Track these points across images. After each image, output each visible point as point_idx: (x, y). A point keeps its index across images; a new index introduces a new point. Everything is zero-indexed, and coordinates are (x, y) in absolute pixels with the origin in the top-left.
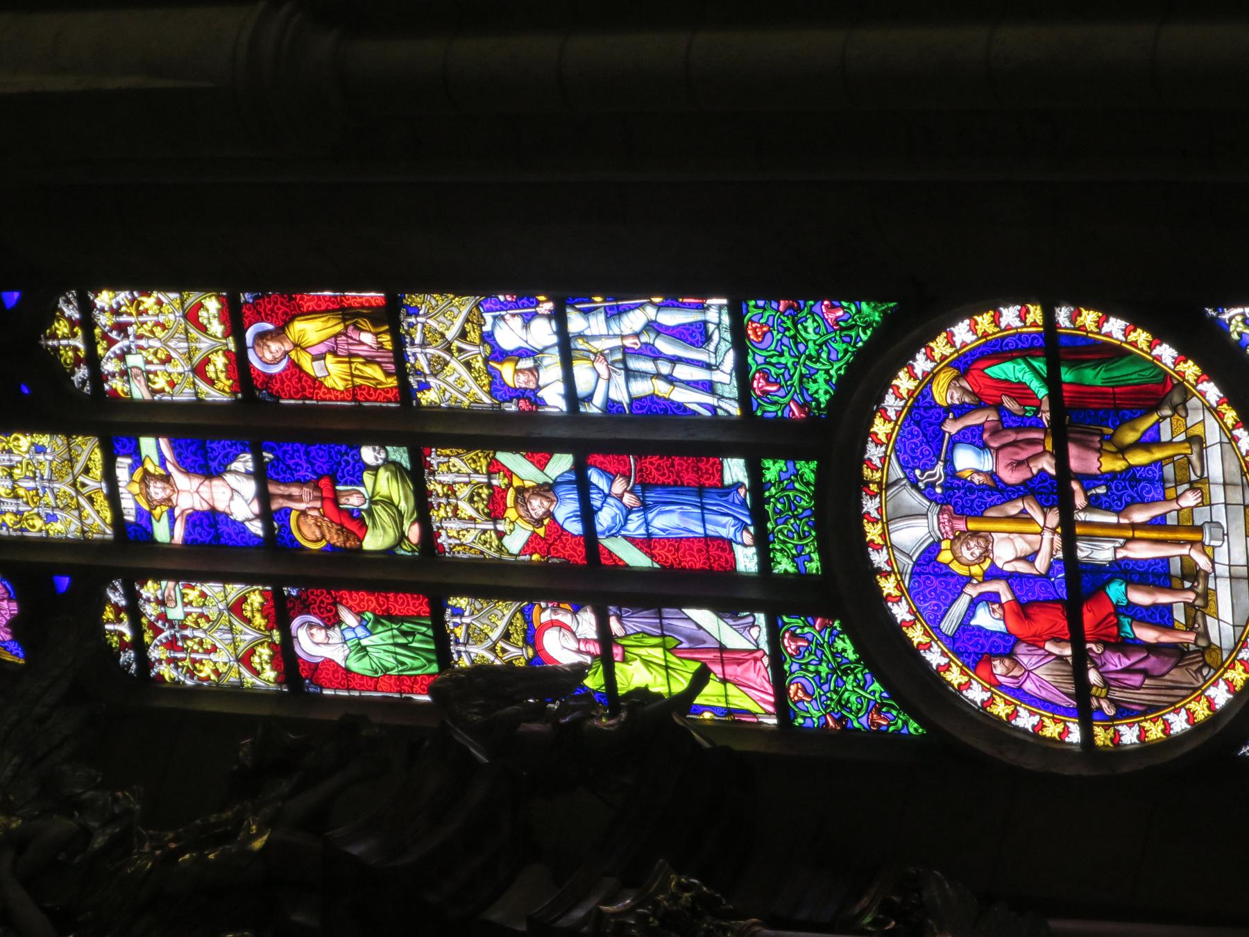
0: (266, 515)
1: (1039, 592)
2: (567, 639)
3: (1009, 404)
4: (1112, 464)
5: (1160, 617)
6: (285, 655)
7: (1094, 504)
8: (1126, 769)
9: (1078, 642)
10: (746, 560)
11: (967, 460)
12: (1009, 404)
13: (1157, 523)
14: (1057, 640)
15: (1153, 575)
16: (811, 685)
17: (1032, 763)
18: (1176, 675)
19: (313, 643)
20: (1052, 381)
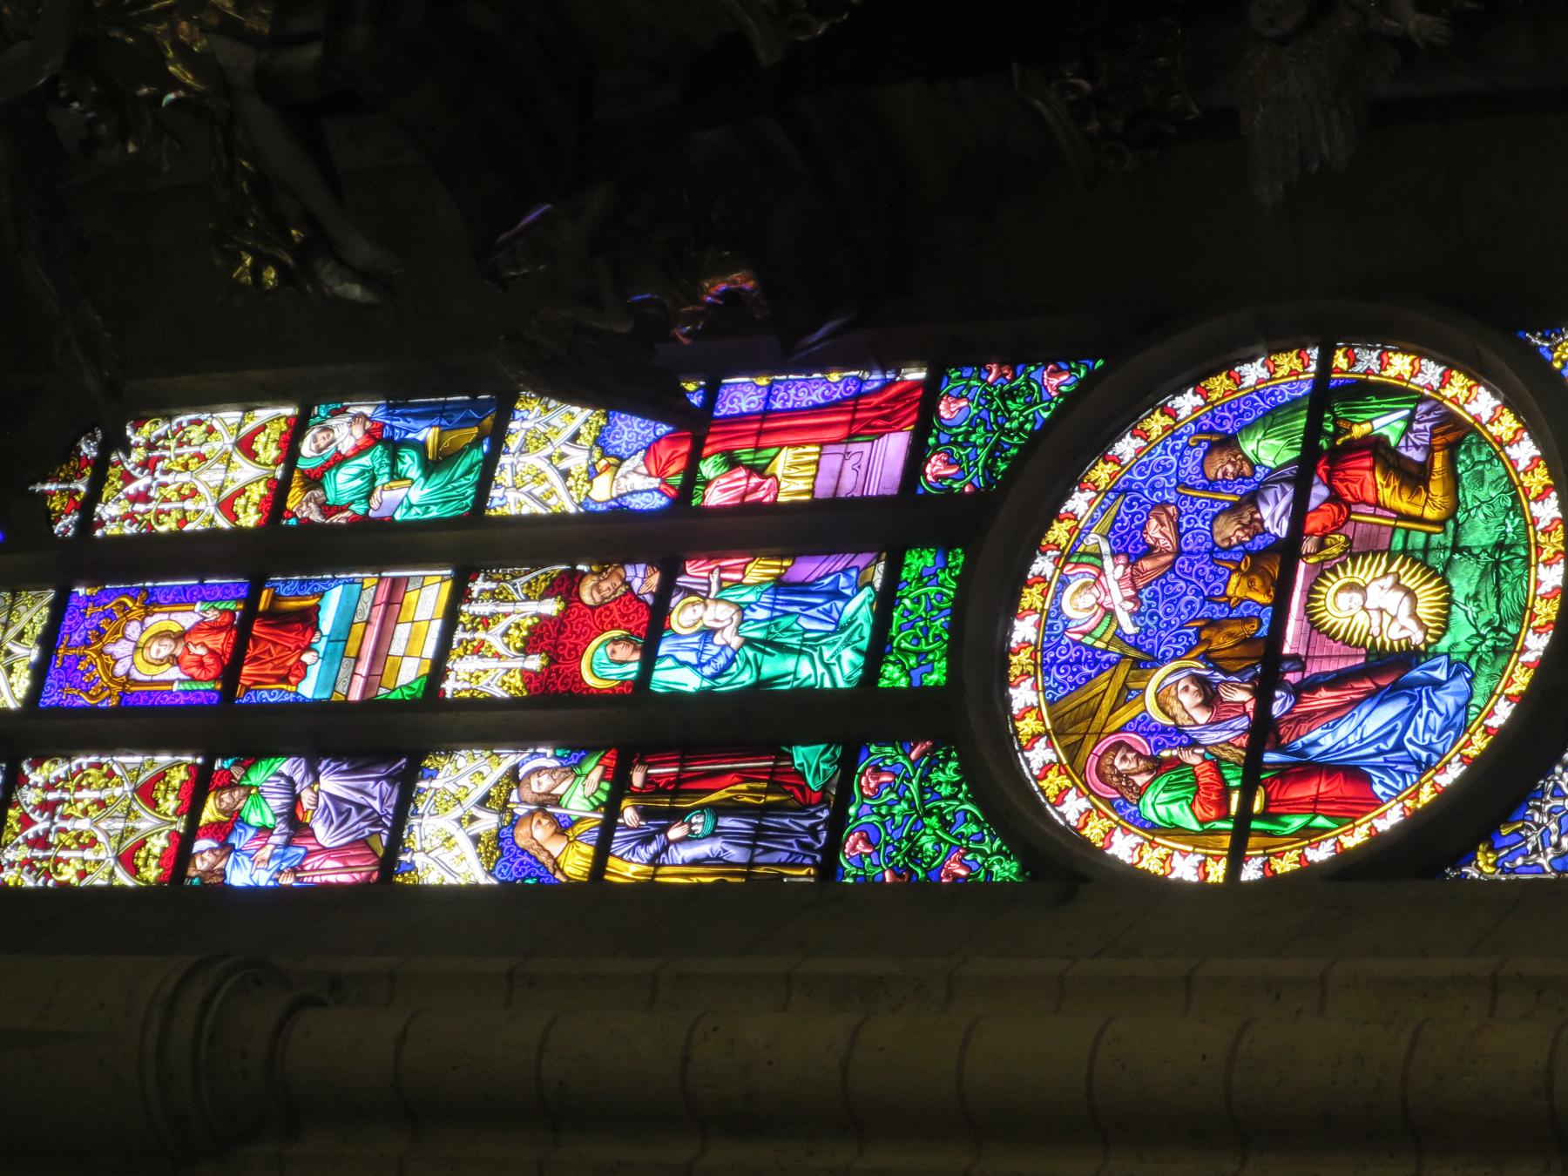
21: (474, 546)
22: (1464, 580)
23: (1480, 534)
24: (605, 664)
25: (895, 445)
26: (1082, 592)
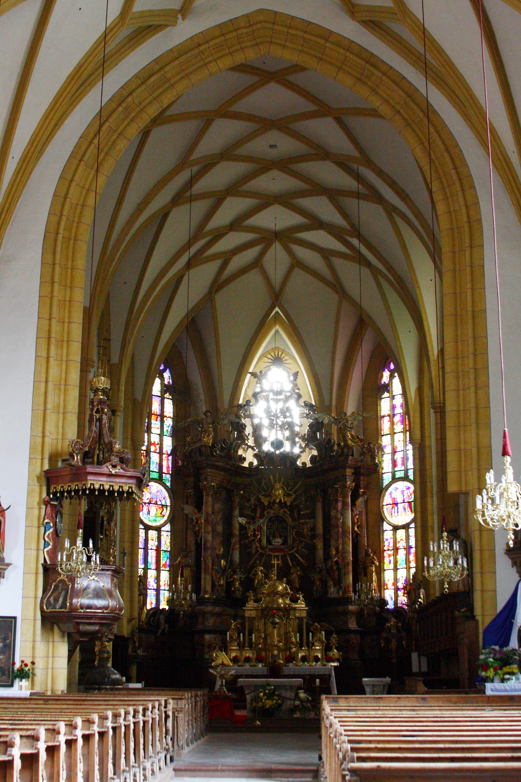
2: (388, 450)
6: (384, 417)
10: (396, 469)
11: (405, 493)
19: (387, 419)
21: (161, 435)
22: (154, 518)
23: (157, 519)
24: (153, 448)
25: (166, 472)
26: (155, 487)
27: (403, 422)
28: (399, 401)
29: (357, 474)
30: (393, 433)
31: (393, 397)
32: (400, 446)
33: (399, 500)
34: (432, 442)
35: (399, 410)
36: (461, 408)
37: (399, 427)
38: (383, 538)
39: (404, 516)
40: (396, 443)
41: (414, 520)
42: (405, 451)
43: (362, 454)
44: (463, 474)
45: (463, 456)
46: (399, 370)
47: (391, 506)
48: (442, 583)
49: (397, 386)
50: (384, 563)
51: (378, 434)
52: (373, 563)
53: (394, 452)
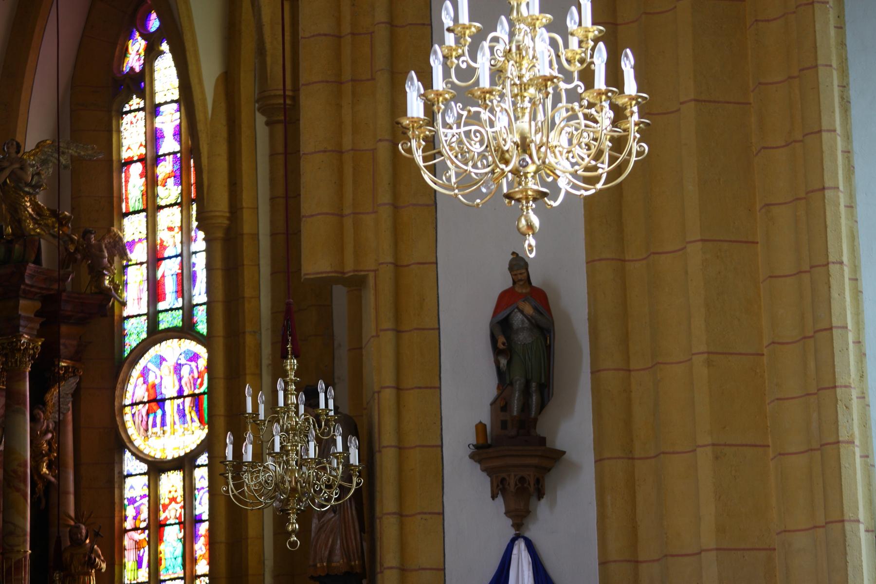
0: (165, 155)
1: (158, 391)
3: (199, 380)
4: (187, 412)
5: (154, 425)
6: (130, 162)
7: (179, 406)
8: (118, 419)
9: (149, 402)
10: (161, 306)
11: (185, 371)
12: (199, 380)
13: (175, 423)
14: (148, 396)
15: (163, 424)
16: (135, 325)
17: (117, 393)
18: (142, 430)
19: (136, 169)
20: (204, 393)
27: (180, 176)
28: (169, 120)
29: (50, 316)
30: (152, 208)
31: (154, 110)
32: (171, 242)
33: (169, 389)
34: (260, 223)
35: (169, 145)
36: (346, 28)
37: (169, 192)
38: (122, 497)
39: (182, 436)
40: (162, 235)
41: (205, 446)
42: (185, 256)
43: (67, 261)
44: (348, 222)
45: (348, 170)
46: (175, 34)
47: (143, 409)
48: (281, 518)
49: (166, 78)
50: (122, 566)
51: (112, 210)
52: (92, 564)
53: (155, 258)
